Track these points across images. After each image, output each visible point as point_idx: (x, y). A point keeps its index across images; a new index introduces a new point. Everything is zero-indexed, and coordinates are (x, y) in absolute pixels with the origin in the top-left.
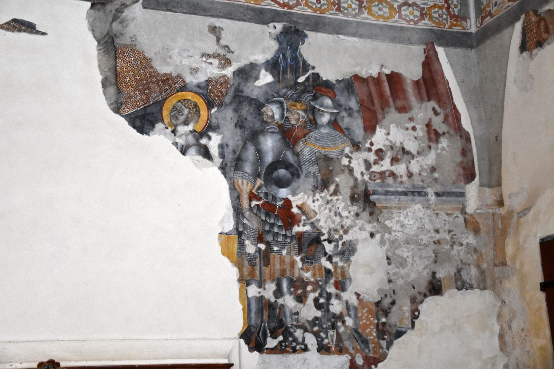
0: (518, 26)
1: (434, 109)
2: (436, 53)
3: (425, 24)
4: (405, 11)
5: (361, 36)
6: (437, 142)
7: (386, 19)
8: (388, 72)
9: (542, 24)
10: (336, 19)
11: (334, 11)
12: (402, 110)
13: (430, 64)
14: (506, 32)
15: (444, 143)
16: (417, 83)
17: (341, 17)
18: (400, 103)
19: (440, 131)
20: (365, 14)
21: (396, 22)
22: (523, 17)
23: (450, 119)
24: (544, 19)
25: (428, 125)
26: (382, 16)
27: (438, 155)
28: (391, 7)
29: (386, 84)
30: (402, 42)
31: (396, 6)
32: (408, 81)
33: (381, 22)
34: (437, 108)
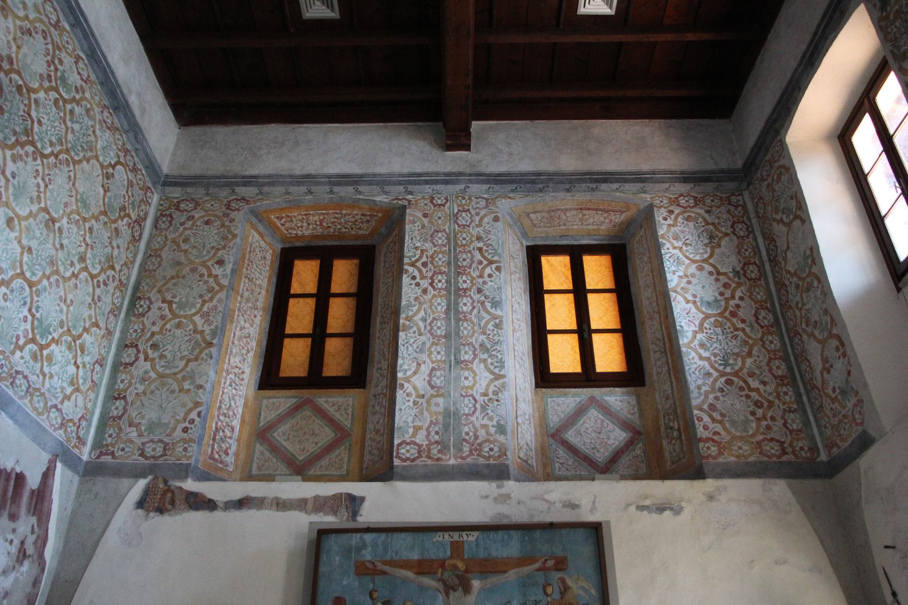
0: (142, 483)
1: (33, 526)
2: (55, 466)
3: (60, 434)
4: (54, 414)
5: (16, 422)
6: (21, 564)
7: (39, 414)
8: (18, 470)
9: (169, 495)
10: (7, 393)
11: (8, 384)
12: (13, 517)
13: (47, 476)
14: (126, 482)
15: (26, 566)
16: (33, 491)
17: (10, 392)
18: (14, 509)
19: (28, 553)
20: (27, 401)
21: (43, 420)
22: (150, 477)
23: (40, 541)
24: (173, 492)
25: (22, 543)
26: (36, 409)
27: (16, 579)
28: (46, 403)
29: (12, 483)
30: (39, 444)
31: (50, 404)
32: (28, 488)
33: (34, 415)
34: (35, 526)
